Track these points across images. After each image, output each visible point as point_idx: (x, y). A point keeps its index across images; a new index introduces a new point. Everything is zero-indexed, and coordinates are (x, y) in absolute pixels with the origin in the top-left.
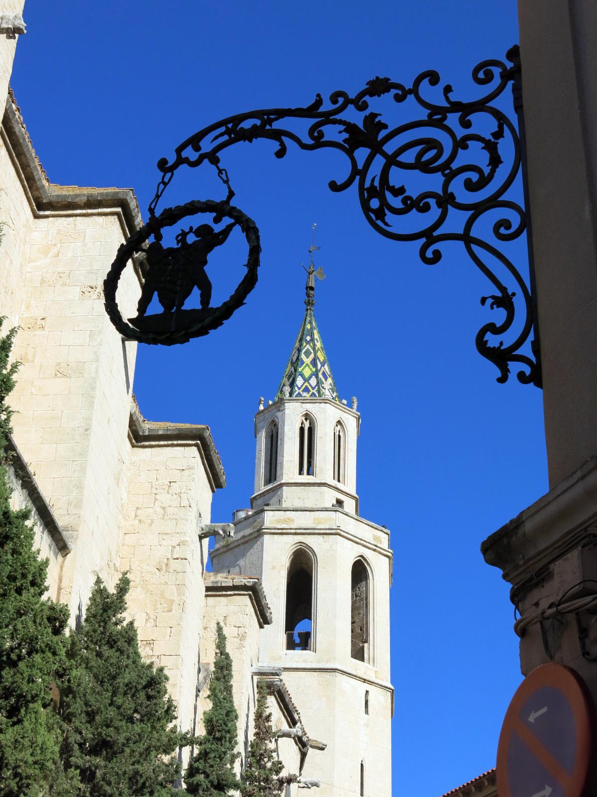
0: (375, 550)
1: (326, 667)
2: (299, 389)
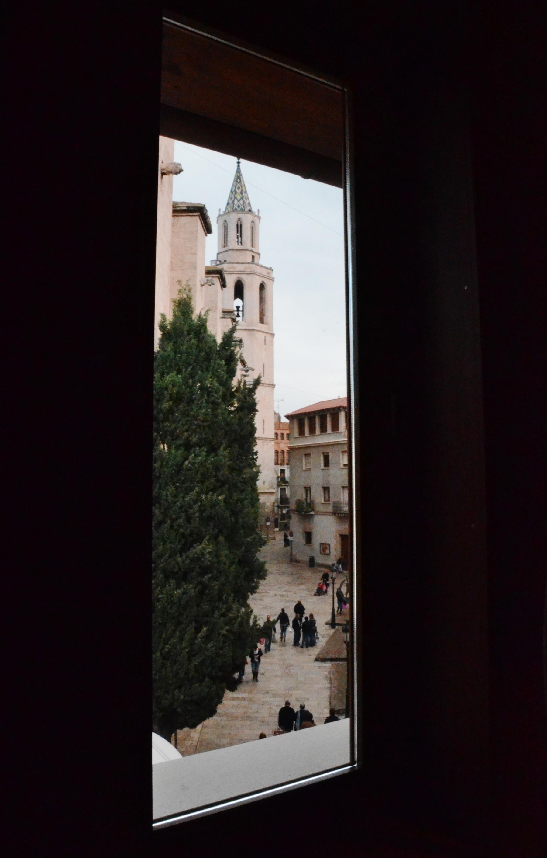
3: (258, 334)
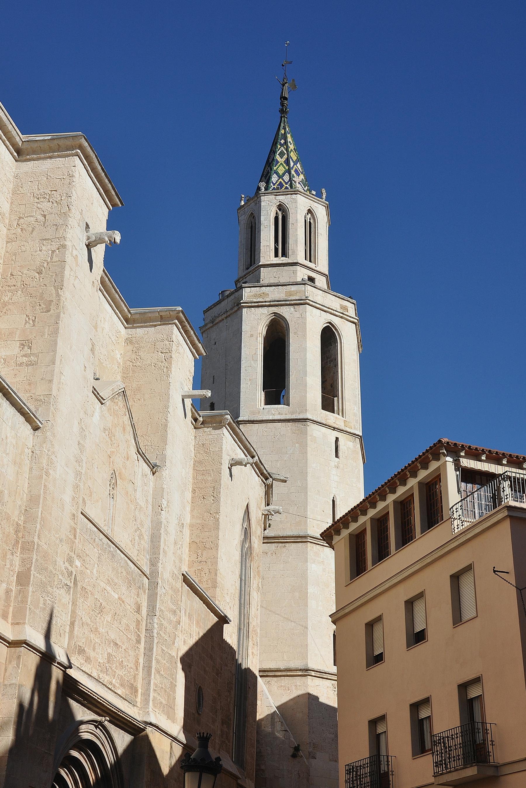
0: (341, 317)
1: (299, 417)
2: (274, 185)
3: (314, 430)
